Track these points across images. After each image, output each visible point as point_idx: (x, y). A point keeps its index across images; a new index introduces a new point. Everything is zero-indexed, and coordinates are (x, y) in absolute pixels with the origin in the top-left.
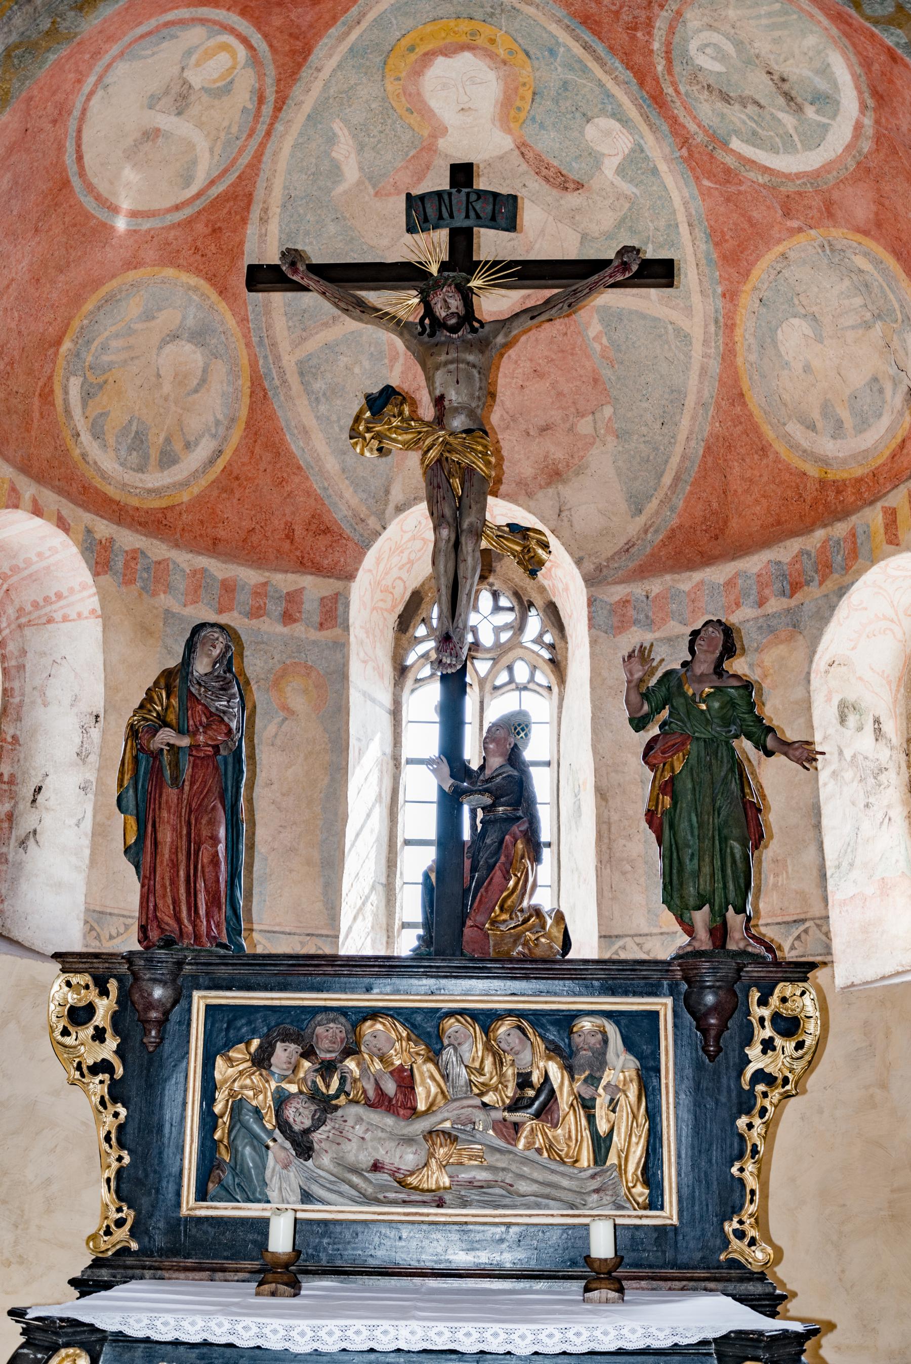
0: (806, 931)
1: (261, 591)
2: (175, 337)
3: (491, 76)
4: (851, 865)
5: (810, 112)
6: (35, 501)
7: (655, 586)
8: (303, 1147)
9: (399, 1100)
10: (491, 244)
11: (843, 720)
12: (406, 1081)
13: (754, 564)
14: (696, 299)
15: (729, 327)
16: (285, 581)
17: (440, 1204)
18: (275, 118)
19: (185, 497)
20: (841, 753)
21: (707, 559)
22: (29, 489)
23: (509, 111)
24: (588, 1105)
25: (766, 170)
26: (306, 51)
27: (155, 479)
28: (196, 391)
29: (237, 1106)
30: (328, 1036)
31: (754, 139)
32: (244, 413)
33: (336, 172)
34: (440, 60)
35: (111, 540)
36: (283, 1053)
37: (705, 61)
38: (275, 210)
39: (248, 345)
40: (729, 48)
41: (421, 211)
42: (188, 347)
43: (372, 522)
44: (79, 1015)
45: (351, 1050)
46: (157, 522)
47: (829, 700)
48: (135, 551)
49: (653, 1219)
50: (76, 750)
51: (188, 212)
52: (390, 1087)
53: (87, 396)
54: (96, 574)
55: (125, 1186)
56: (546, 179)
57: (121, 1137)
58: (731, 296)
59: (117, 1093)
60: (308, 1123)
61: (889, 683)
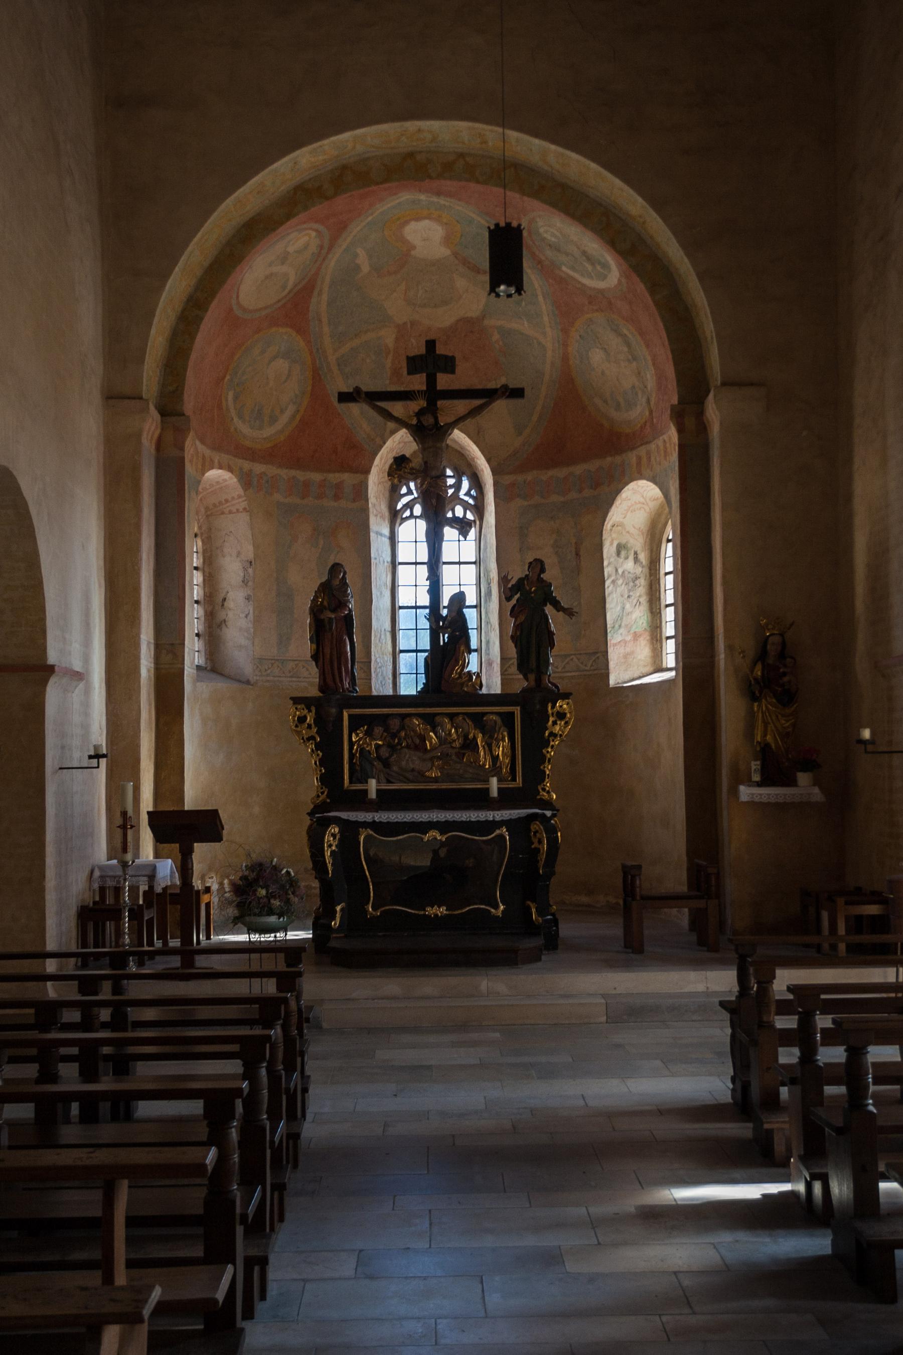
0: (598, 658)
2: (275, 358)
3: (439, 228)
4: (620, 626)
5: (598, 268)
6: (219, 462)
7: (529, 476)
8: (386, 764)
9: (419, 746)
10: (444, 381)
11: (618, 554)
12: (423, 739)
13: (578, 469)
14: (548, 330)
15: (565, 345)
16: (334, 478)
17: (437, 782)
18: (328, 253)
19: (282, 438)
20: (617, 570)
22: (217, 457)
23: (447, 240)
24: (490, 746)
25: (579, 282)
26: (345, 227)
27: (268, 432)
28: (285, 381)
29: (362, 751)
30: (395, 724)
31: (573, 268)
32: (309, 388)
33: (358, 268)
34: (413, 223)
35: (251, 471)
36: (378, 730)
37: (548, 236)
38: (326, 289)
39: (311, 353)
40: (558, 234)
41: (414, 364)
42: (281, 361)
43: (378, 440)
44: (302, 720)
45: (402, 728)
46: (270, 455)
47: (612, 544)
48: (261, 474)
49: (512, 785)
50: (241, 579)
51: (283, 302)
52: (418, 741)
53: (236, 398)
54: (245, 490)
55: (323, 780)
56: (468, 267)
57: (322, 762)
58: (565, 331)
59: (318, 747)
60: (387, 755)
61: (643, 534)
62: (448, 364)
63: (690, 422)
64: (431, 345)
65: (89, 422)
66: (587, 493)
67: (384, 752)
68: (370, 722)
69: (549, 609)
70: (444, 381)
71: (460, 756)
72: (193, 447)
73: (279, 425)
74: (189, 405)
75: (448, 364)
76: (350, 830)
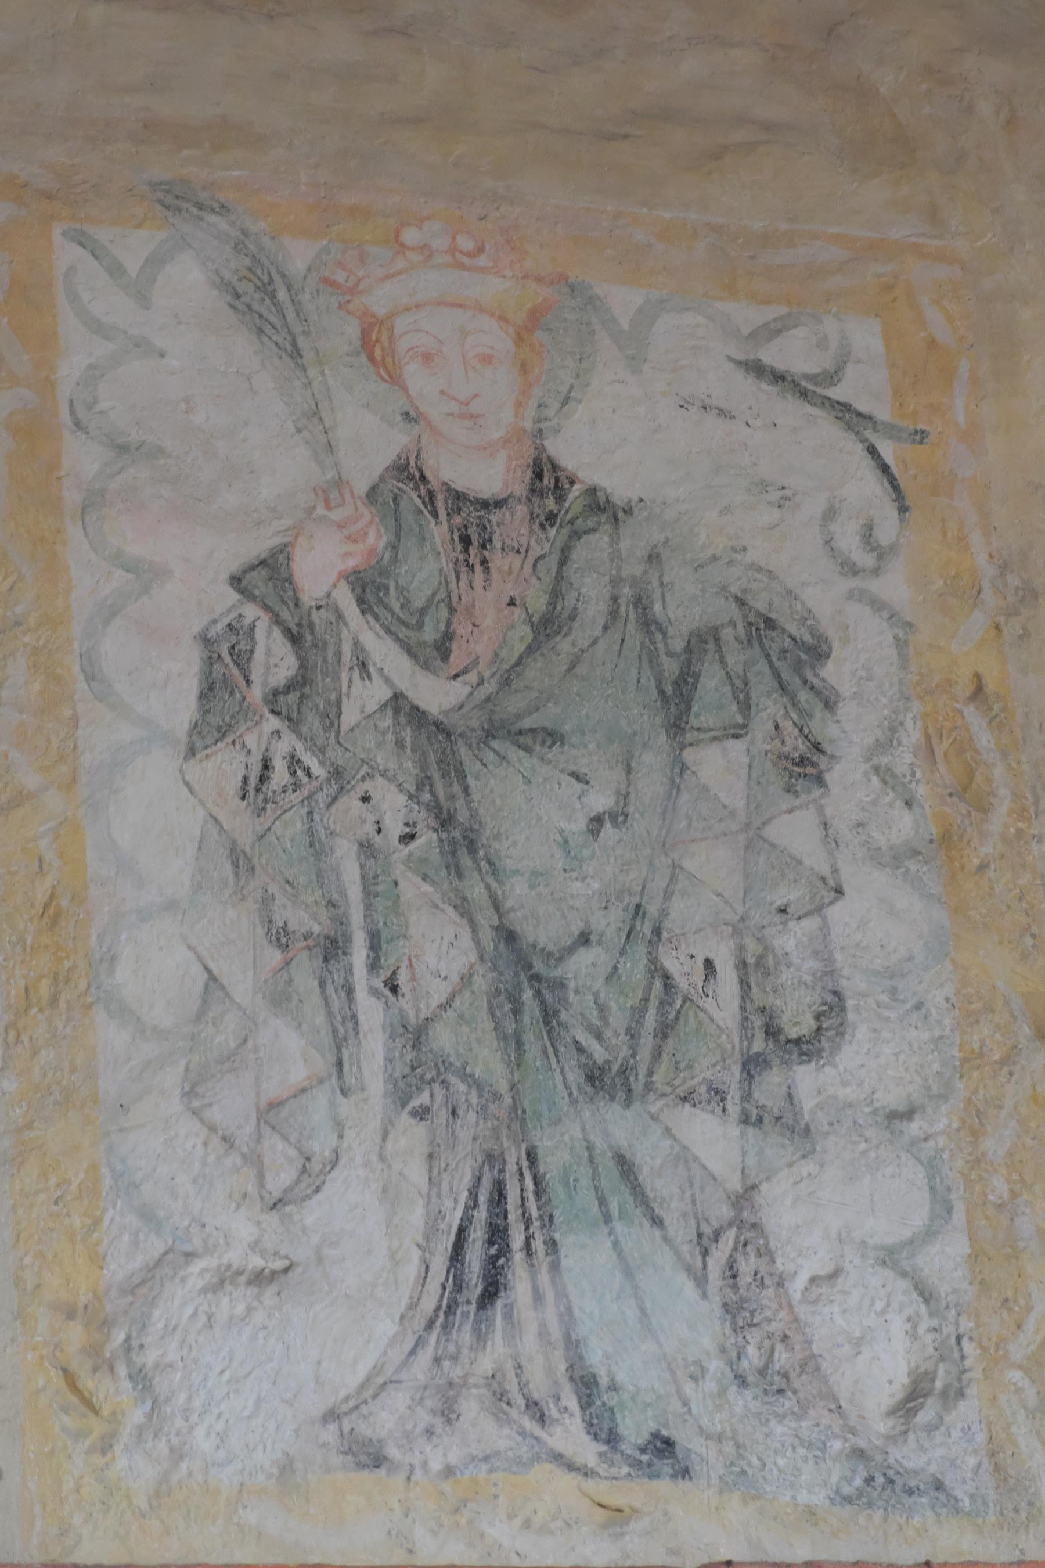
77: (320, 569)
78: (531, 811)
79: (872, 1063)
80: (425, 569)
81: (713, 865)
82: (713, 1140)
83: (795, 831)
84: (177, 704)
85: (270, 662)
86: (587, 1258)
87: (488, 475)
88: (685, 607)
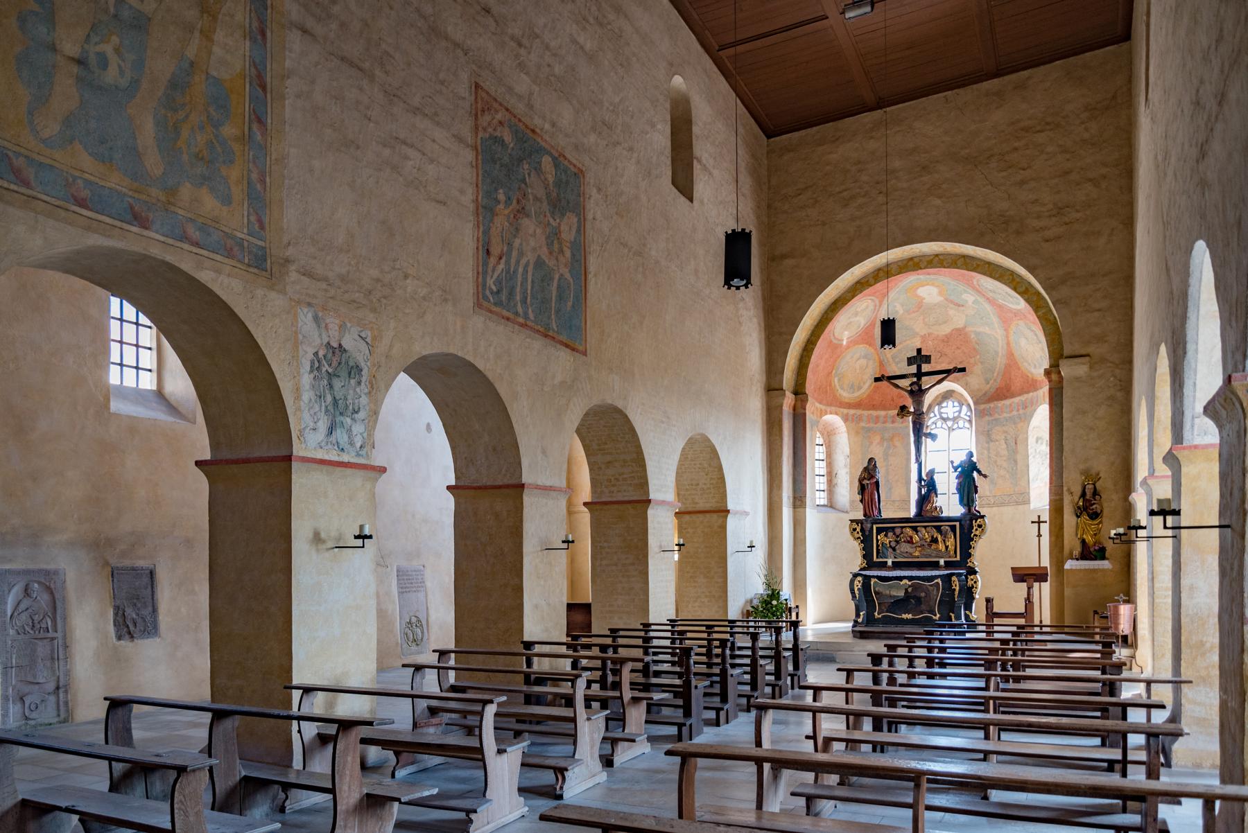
1: (885, 417)
7: (992, 405)
10: (925, 368)
13: (1016, 400)
21: (1006, 398)
22: (828, 409)
27: (856, 394)
41: (910, 361)
46: (858, 405)
62: (927, 359)
63: (1054, 377)
64: (919, 351)
65: (755, 404)
66: (1021, 412)
67: (893, 544)
68: (886, 530)
69: (975, 474)
70: (925, 368)
71: (930, 546)
72: (812, 408)
73: (862, 391)
74: (810, 387)
75: (927, 359)
76: (867, 579)
77: (321, 354)
78: (337, 384)
79: (362, 415)
80: (330, 355)
81: (351, 392)
82: (349, 420)
83: (358, 390)
84: (308, 368)
85: (316, 367)
86: (339, 431)
87: (335, 345)
88: (351, 364)
